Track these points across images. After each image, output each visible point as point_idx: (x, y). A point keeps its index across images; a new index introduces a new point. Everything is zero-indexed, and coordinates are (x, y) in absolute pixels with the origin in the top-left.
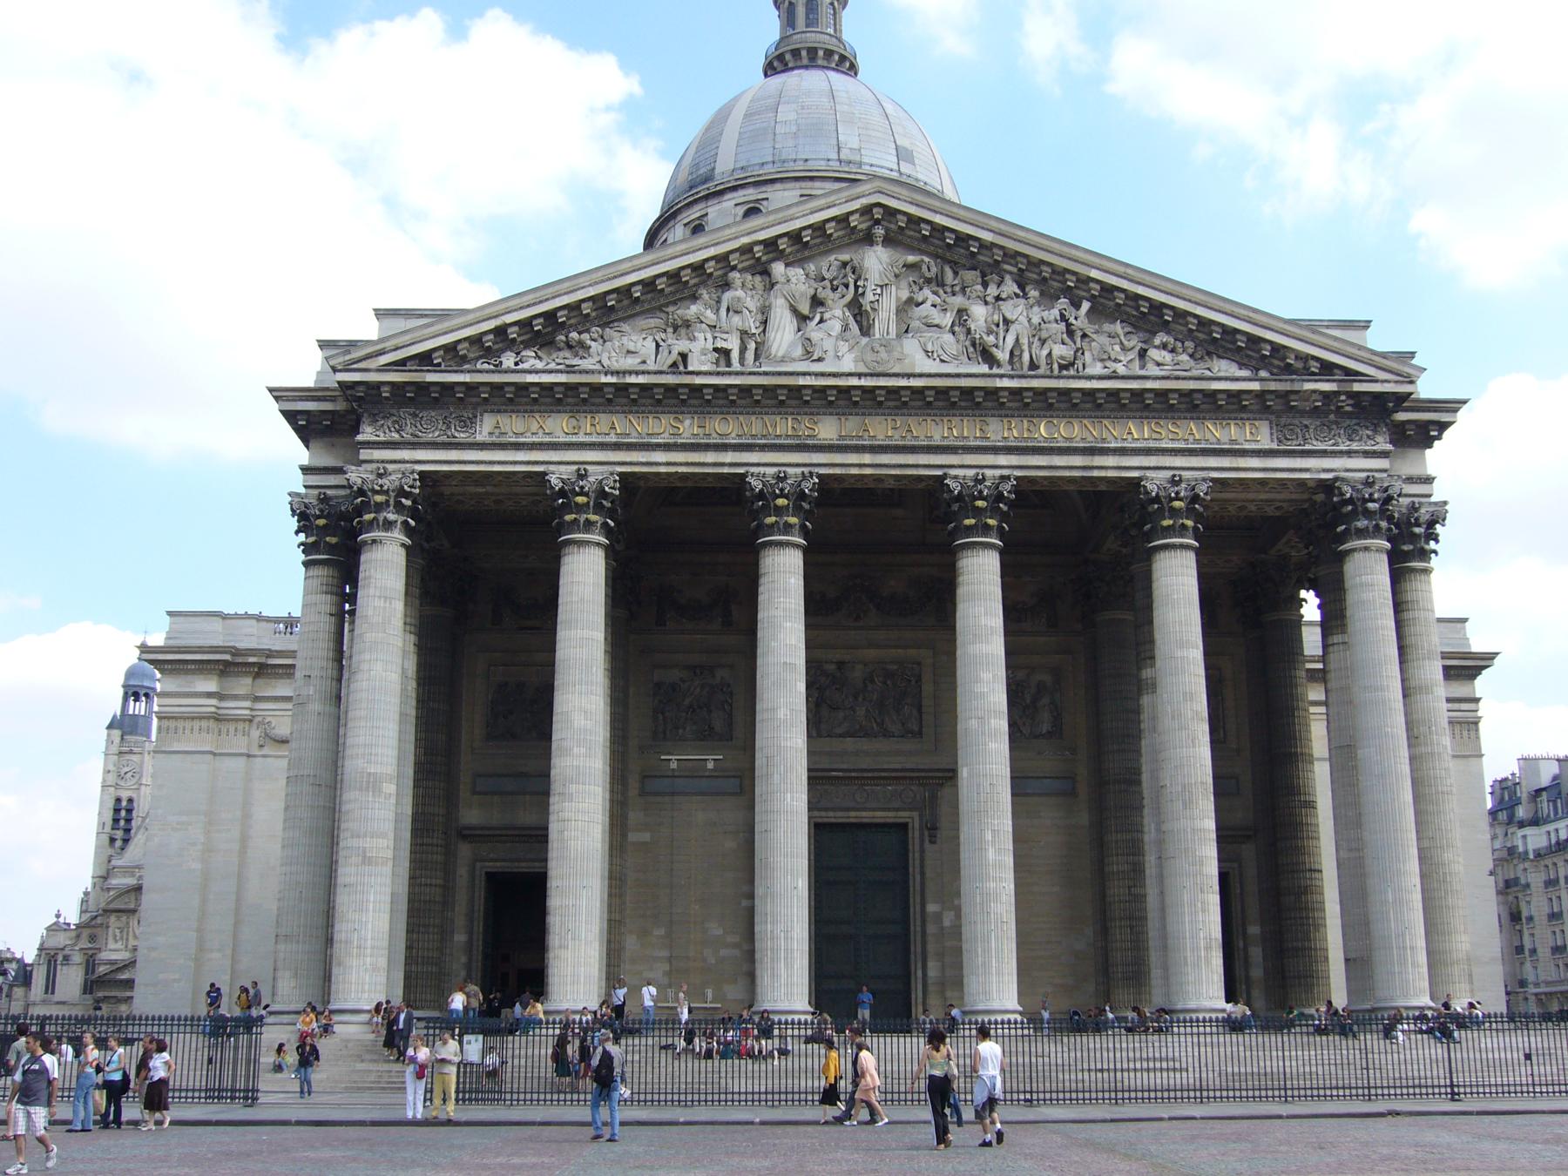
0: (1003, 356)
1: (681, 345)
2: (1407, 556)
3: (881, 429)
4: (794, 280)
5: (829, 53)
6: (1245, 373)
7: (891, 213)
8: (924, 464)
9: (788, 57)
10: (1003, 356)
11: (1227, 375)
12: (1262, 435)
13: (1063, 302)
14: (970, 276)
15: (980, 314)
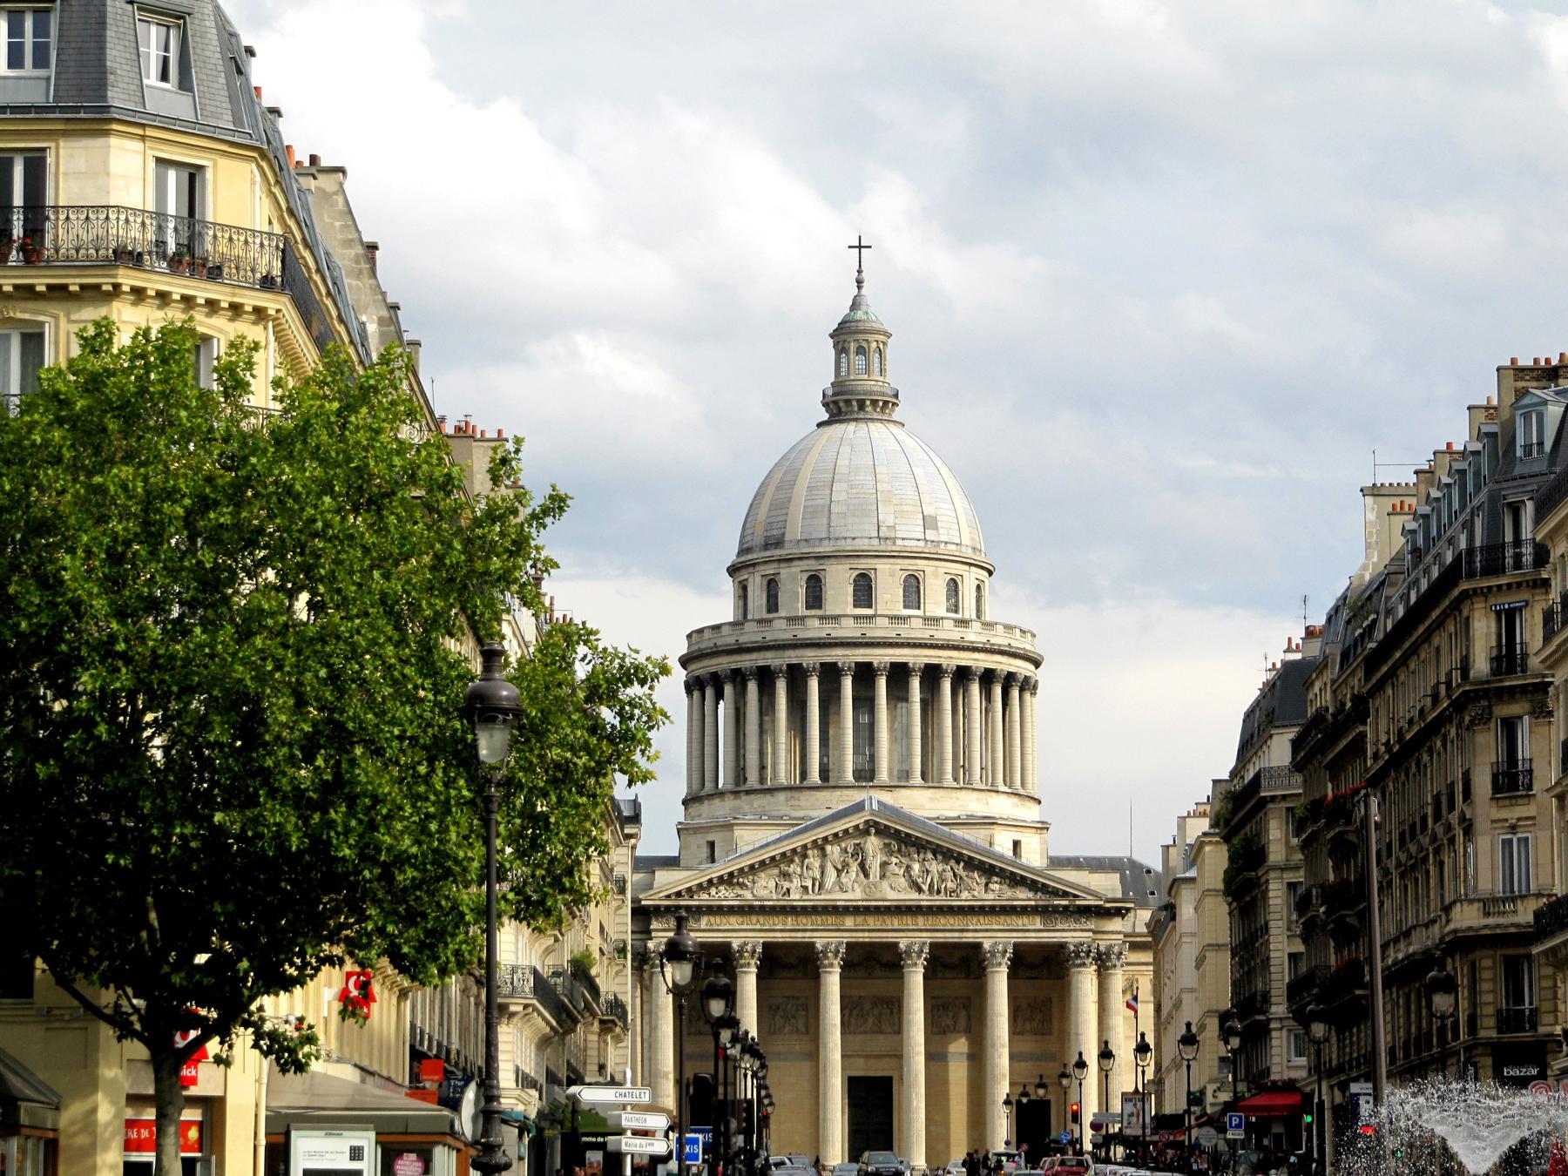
0: (925, 888)
1: (786, 885)
2: (1108, 968)
3: (872, 922)
4: (833, 851)
5: (874, 403)
6: (1031, 895)
7: (876, 823)
8: (889, 937)
9: (841, 404)
10: (925, 888)
11: (1023, 897)
12: (1037, 923)
13: (952, 863)
14: (912, 850)
15: (916, 867)
